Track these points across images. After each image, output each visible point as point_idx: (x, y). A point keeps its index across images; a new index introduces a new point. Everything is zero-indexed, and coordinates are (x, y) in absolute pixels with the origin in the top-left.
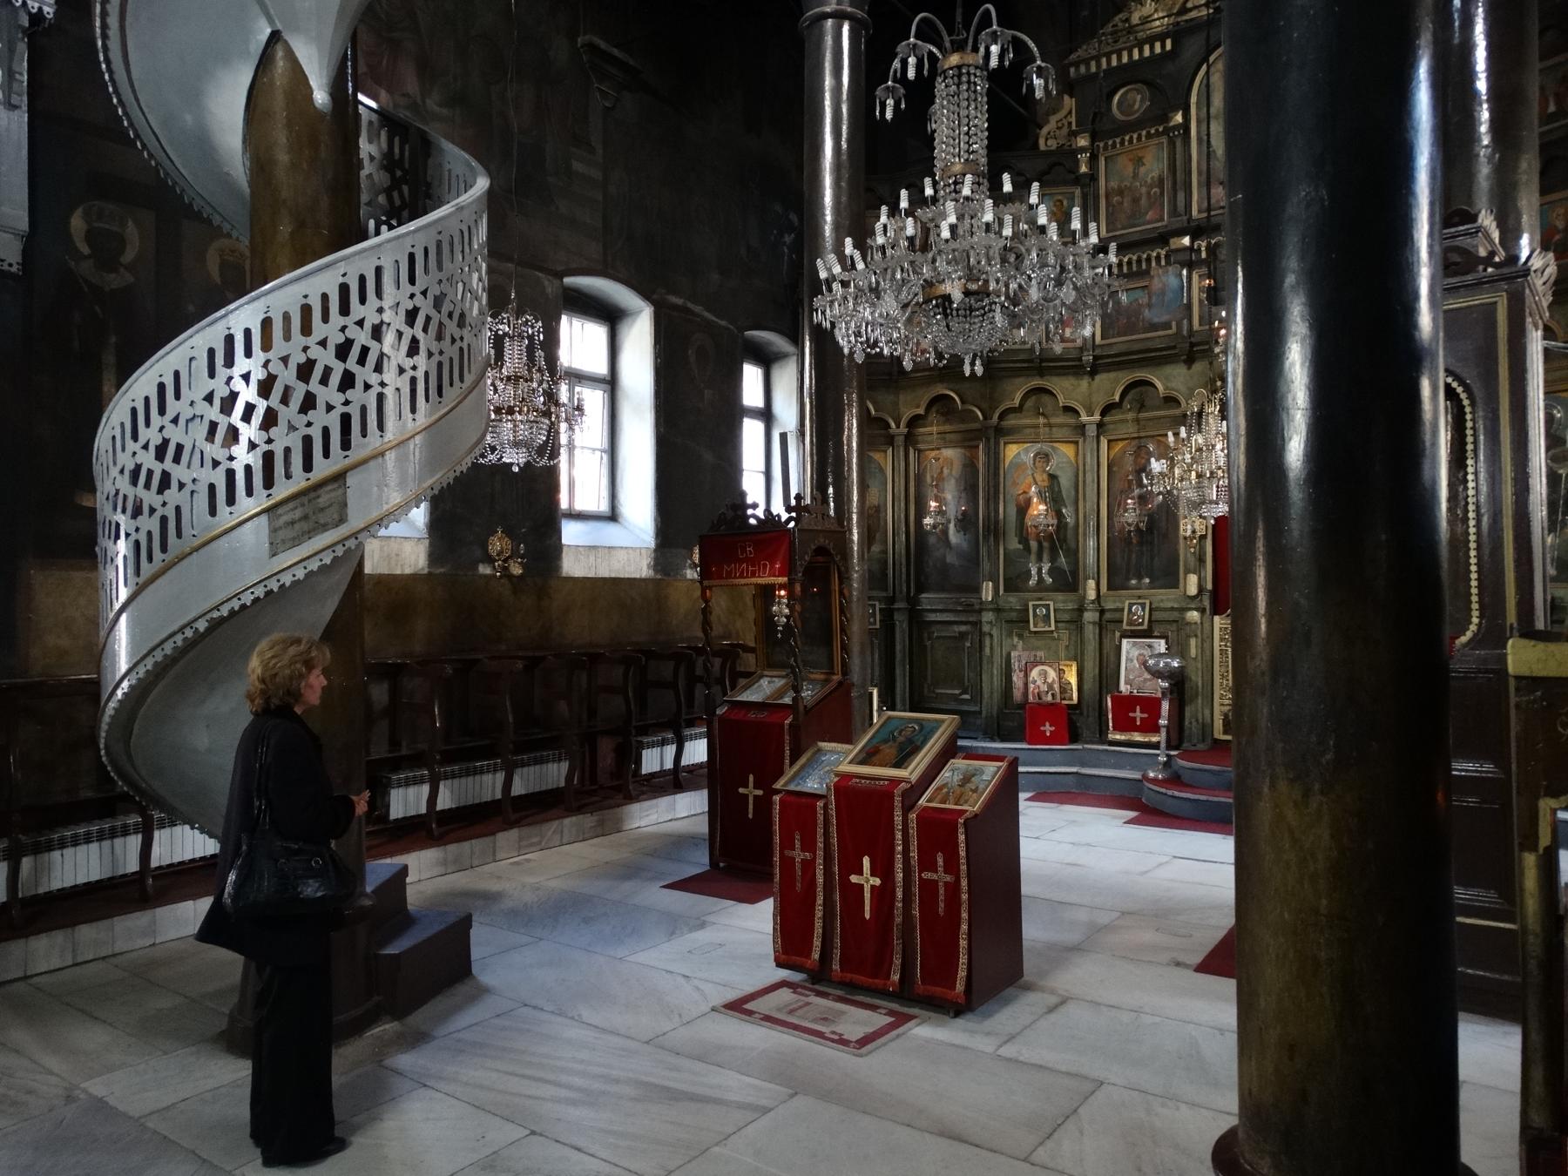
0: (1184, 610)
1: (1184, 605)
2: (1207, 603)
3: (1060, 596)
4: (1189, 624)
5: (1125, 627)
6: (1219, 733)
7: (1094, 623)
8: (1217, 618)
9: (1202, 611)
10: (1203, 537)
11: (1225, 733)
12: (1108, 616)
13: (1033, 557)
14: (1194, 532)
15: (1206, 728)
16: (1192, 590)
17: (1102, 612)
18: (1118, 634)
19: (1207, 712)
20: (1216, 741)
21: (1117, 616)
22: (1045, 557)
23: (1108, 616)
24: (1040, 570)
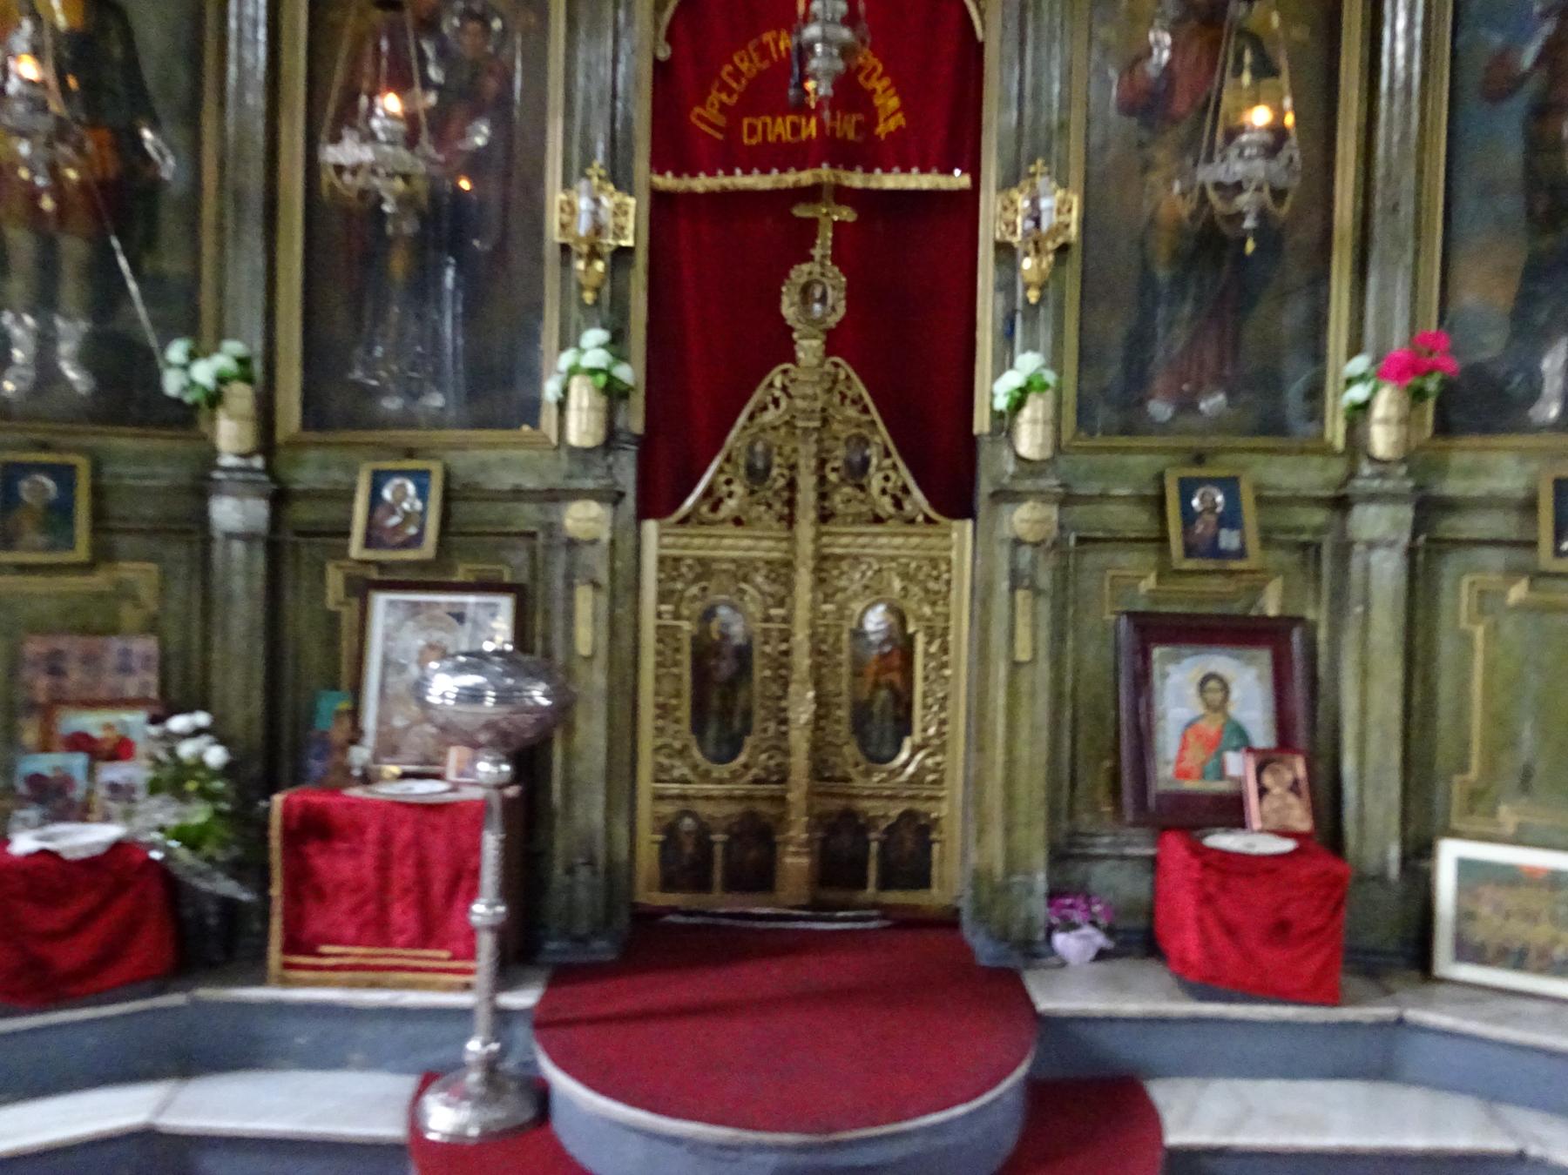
0: (555, 496)
1: (555, 480)
2: (626, 472)
3: (123, 443)
4: (572, 544)
5: (356, 548)
6: (650, 896)
7: (248, 538)
8: (651, 527)
9: (613, 498)
10: (622, 256)
11: (668, 884)
12: (303, 513)
13: (17, 287)
14: (598, 229)
15: (616, 877)
16: (582, 427)
17: (280, 498)
18: (335, 579)
19: (621, 831)
20: (646, 918)
21: (331, 512)
22: (70, 290)
23: (303, 513)
24: (46, 342)
